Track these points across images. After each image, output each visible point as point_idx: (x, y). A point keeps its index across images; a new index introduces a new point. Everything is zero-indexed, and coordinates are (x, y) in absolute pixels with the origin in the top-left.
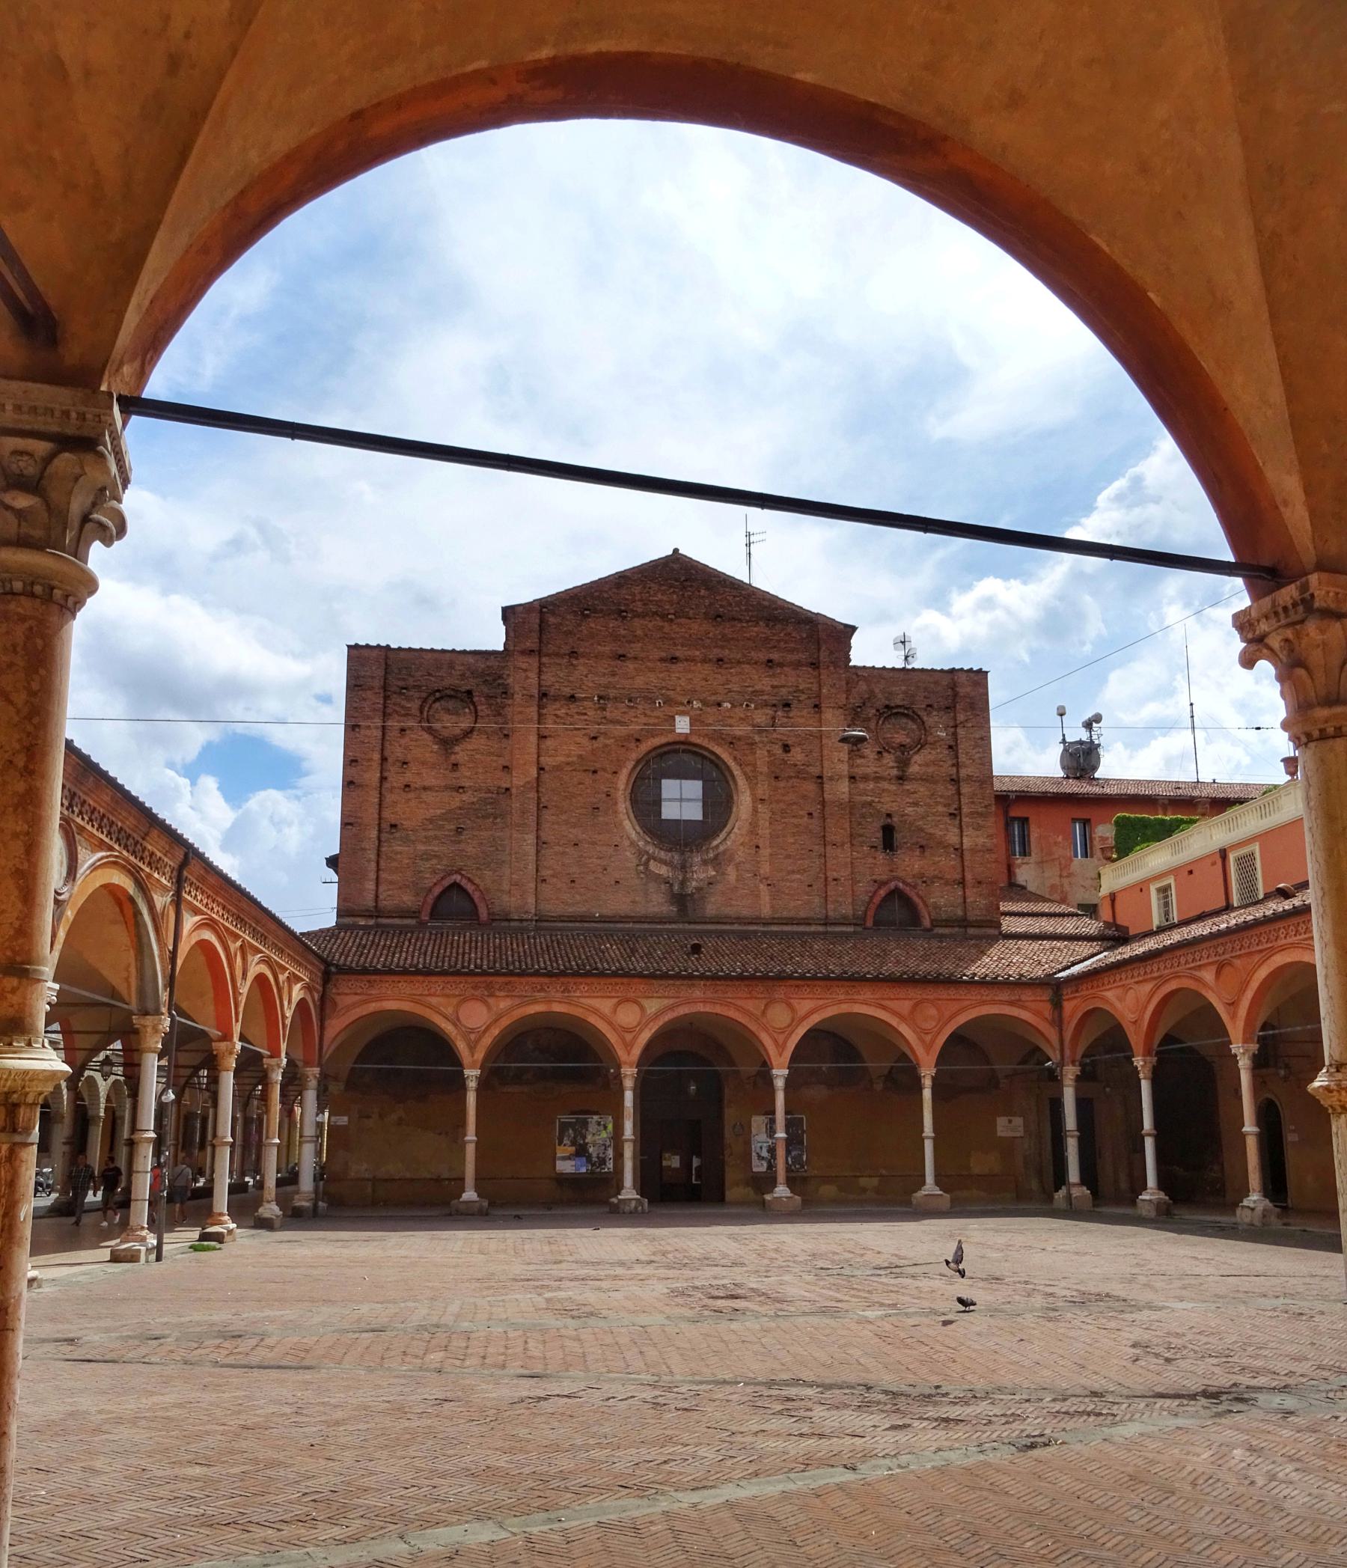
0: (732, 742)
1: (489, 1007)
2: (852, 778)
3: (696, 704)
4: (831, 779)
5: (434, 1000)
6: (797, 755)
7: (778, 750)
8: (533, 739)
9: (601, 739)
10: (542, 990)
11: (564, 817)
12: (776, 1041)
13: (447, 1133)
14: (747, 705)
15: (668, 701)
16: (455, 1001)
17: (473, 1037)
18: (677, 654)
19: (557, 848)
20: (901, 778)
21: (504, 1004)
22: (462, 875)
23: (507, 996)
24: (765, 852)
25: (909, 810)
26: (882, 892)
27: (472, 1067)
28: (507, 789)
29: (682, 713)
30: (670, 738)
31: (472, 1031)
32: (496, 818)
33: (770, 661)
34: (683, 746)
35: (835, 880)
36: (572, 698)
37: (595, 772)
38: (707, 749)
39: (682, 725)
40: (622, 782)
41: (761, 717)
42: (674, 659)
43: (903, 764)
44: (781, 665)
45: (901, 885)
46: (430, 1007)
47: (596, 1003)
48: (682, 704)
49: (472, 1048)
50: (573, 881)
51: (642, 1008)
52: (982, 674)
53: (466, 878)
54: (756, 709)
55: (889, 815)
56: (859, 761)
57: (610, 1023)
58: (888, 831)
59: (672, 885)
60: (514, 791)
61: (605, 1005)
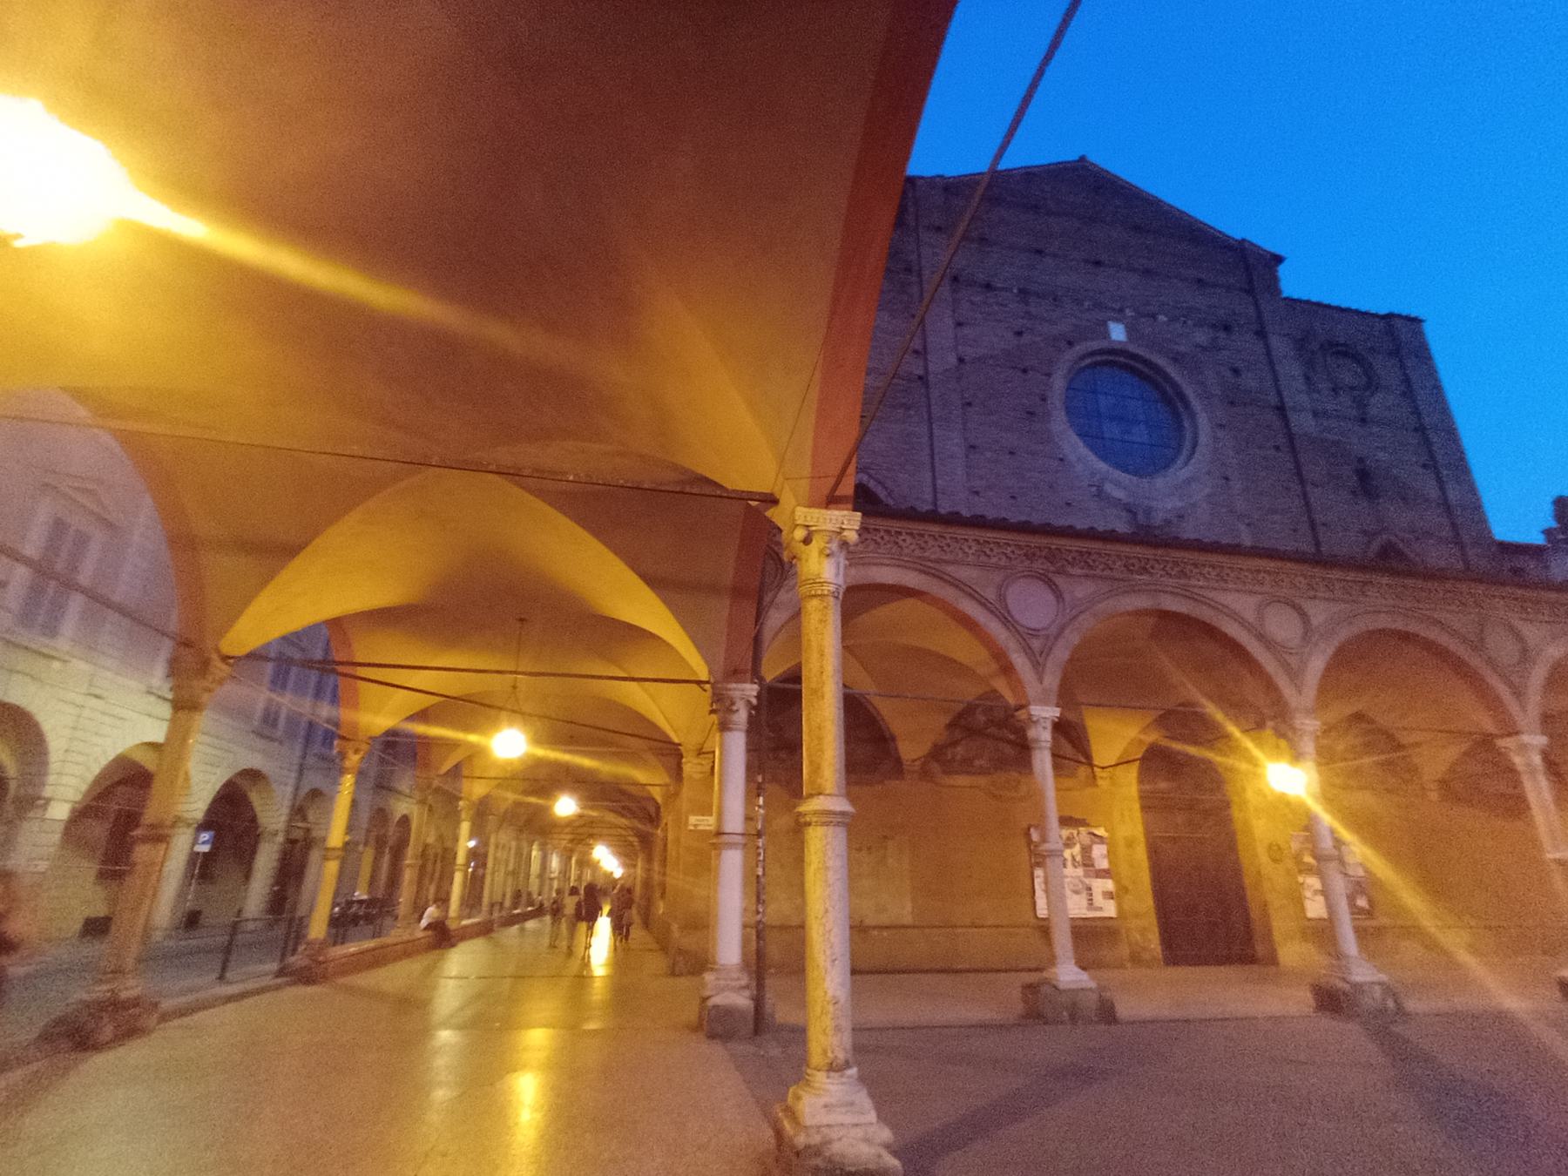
0: (1176, 359)
1: (1059, 596)
2: (1315, 414)
3: (1129, 313)
4: (1294, 409)
5: (964, 573)
6: (1249, 381)
7: (1228, 374)
8: (949, 322)
9: (1026, 338)
10: (1144, 570)
11: (994, 418)
12: (1511, 685)
13: (869, 848)
14: (1185, 322)
15: (1098, 306)
16: (997, 577)
17: (1036, 644)
18: (1104, 257)
19: (988, 455)
20: (1363, 420)
21: (1080, 590)
22: (870, 476)
23: (1086, 576)
24: (1237, 485)
25: (1381, 455)
26: (1375, 546)
27: (1044, 702)
28: (920, 378)
29: (1117, 320)
30: (1104, 344)
31: (1034, 633)
32: (908, 408)
33: (1199, 281)
34: (1115, 359)
35: (1324, 524)
36: (988, 287)
37: (1025, 371)
38: (1146, 362)
39: (1118, 332)
40: (1059, 383)
41: (1202, 337)
42: (1098, 263)
43: (1361, 404)
44: (1215, 285)
45: (1393, 539)
46: (957, 584)
47: (1231, 600)
48: (1114, 310)
49: (1038, 667)
50: (1013, 497)
51: (1303, 615)
52: (1416, 321)
53: (876, 480)
54: (1195, 325)
55: (1361, 460)
56: (1316, 396)
57: (1260, 637)
58: (1364, 475)
59: (1135, 514)
60: (931, 378)
61: (1244, 604)
